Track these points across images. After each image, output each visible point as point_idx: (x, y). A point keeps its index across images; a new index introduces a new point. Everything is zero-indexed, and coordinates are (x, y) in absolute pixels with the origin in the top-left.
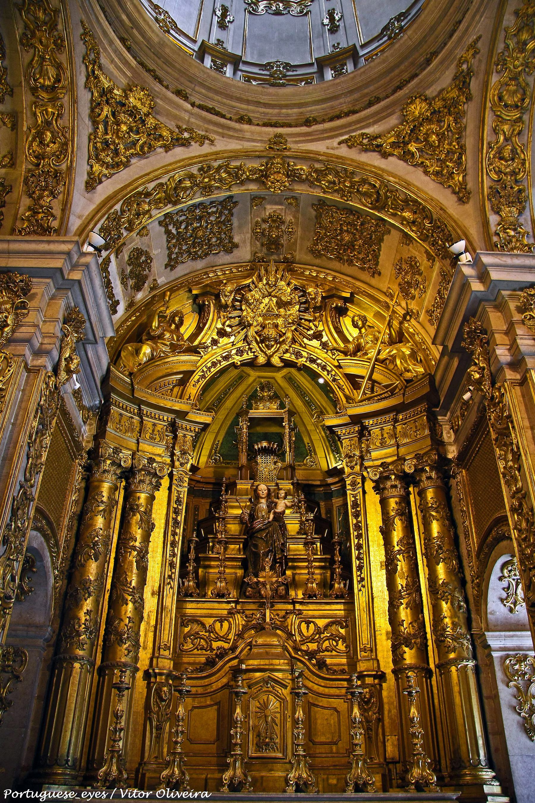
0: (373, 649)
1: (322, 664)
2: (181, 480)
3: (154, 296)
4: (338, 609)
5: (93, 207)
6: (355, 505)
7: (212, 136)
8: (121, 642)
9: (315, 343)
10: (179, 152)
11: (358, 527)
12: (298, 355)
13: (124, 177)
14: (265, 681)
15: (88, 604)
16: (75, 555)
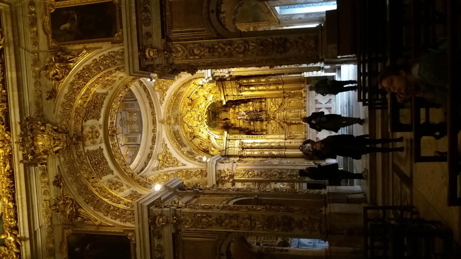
0: (278, 94)
1: (281, 104)
2: (242, 137)
3: (194, 149)
4: (269, 100)
5: (190, 164)
6: (246, 97)
7: (163, 139)
8: (280, 145)
9: (200, 106)
10: (169, 146)
11: (251, 97)
12: (204, 110)
13: (179, 158)
14: (286, 116)
15: (274, 153)
16: (263, 157)
